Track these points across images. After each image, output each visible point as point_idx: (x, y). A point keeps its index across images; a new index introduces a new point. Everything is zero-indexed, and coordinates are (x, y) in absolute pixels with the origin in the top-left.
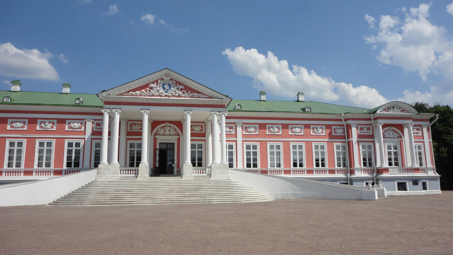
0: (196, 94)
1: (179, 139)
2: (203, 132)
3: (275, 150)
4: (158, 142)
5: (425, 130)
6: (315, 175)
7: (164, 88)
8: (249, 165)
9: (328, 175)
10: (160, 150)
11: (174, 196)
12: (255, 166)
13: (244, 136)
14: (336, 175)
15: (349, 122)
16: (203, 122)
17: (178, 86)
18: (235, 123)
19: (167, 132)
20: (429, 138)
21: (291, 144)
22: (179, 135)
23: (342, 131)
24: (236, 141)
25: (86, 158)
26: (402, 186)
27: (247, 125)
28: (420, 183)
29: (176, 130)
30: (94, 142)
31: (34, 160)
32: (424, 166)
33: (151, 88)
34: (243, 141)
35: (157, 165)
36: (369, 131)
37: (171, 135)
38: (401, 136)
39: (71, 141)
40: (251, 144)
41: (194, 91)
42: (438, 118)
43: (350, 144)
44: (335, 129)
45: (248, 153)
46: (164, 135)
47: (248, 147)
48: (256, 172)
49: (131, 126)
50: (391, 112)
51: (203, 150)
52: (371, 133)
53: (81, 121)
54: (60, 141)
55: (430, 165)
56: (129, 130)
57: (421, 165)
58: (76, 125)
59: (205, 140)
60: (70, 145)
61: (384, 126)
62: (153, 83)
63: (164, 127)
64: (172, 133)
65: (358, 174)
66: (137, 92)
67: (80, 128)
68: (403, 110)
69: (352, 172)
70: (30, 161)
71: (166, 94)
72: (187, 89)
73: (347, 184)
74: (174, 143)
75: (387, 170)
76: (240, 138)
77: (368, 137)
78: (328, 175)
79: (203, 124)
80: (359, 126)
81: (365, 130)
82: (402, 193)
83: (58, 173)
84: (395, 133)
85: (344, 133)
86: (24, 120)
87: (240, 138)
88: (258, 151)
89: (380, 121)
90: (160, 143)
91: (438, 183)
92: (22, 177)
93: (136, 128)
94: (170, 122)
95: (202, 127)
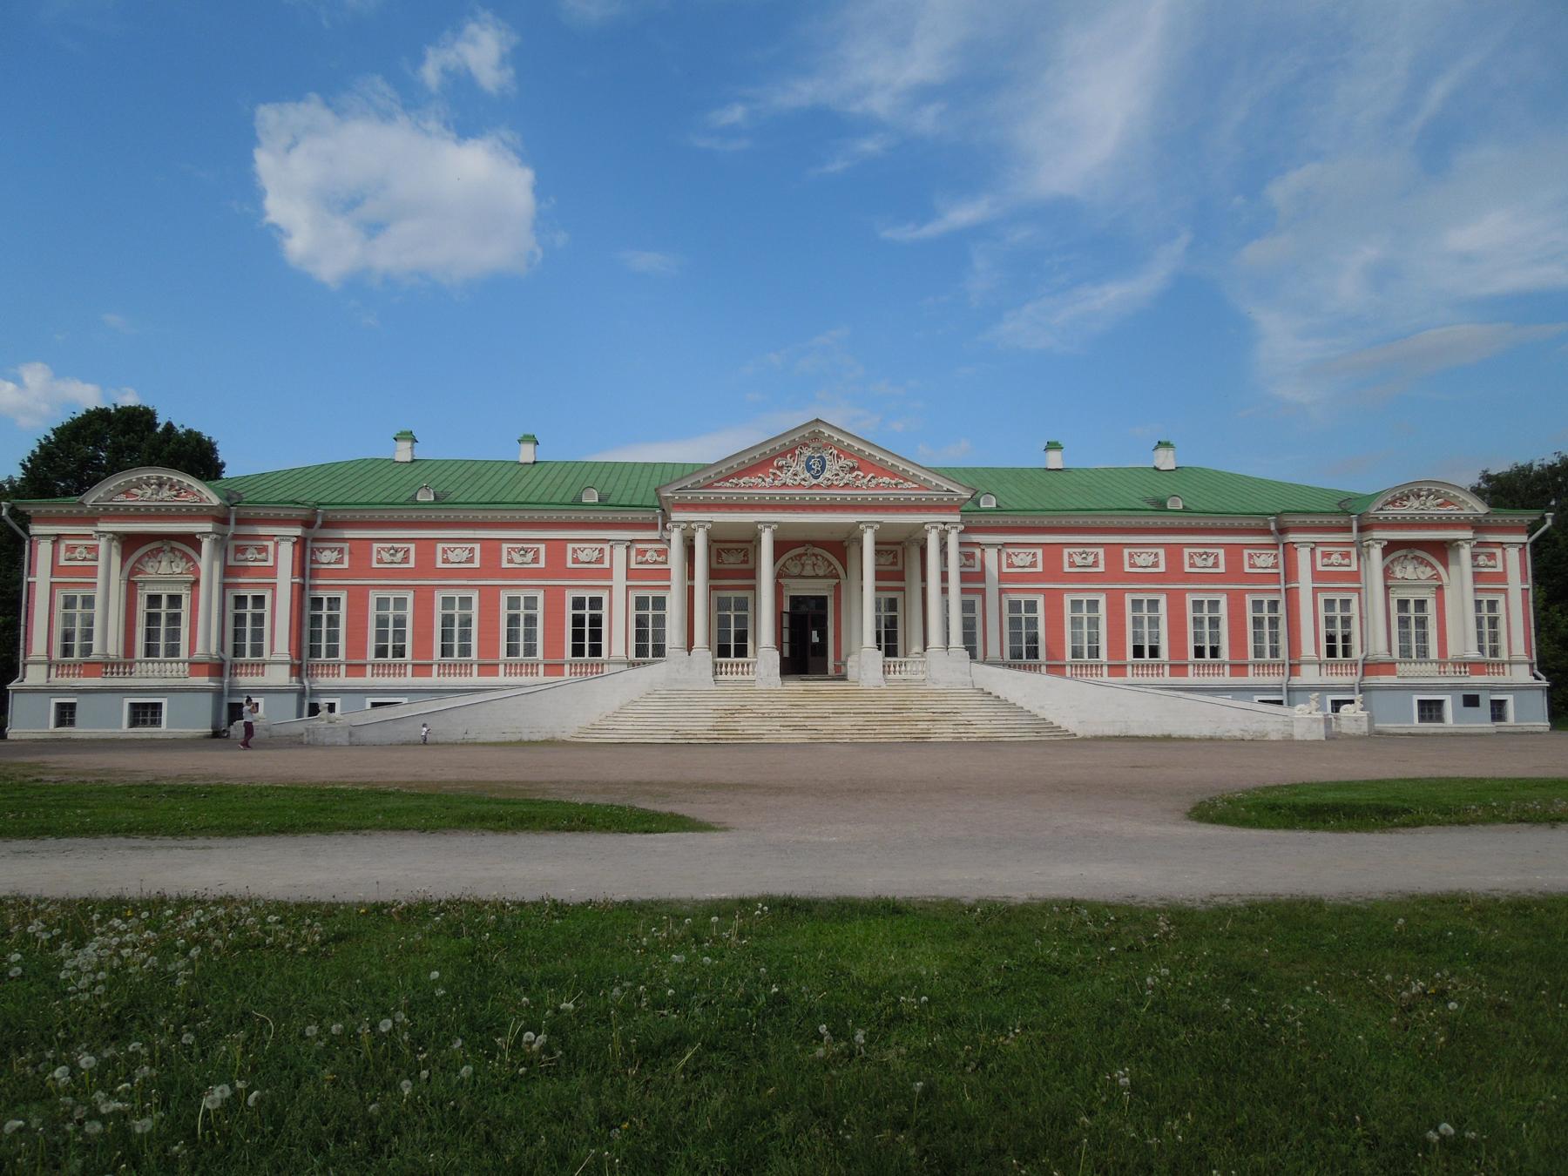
0: (886, 479)
1: (837, 588)
2: (899, 567)
3: (1085, 614)
4: (787, 594)
5: (1513, 554)
7: (809, 468)
8: (1016, 655)
9: (1226, 679)
10: (792, 615)
14: (1251, 679)
15: (1292, 537)
16: (899, 543)
17: (842, 462)
18: (979, 544)
19: (808, 571)
20: (1524, 580)
21: (1128, 598)
22: (837, 577)
23: (1271, 561)
24: (983, 592)
25: (618, 637)
26: (1431, 710)
27: (1010, 551)
28: (1485, 708)
29: (830, 564)
30: (633, 595)
31: (498, 640)
32: (1504, 656)
33: (780, 468)
34: (1002, 591)
35: (786, 654)
36: (1346, 561)
37: (817, 577)
38: (1438, 573)
39: (579, 594)
41: (882, 469)
42: (1549, 522)
43: (1292, 595)
44: (1251, 556)
46: (800, 576)
48: (1036, 668)
49: (719, 555)
50: (1412, 508)
51: (899, 615)
52: (1354, 568)
53: (600, 546)
54: (554, 595)
55: (1519, 649)
56: (715, 566)
57: (1495, 652)
59: (902, 589)
60: (578, 603)
61: (1391, 547)
62: (783, 455)
63: (800, 556)
64: (821, 573)
66: (746, 479)
67: (600, 560)
69: (1294, 669)
70: (488, 645)
71: (815, 482)
72: (864, 464)
73: (1280, 703)
74: (824, 598)
75: (1388, 667)
78: (1226, 679)
79: (899, 548)
80: (1319, 550)
81: (1336, 558)
82: (1431, 727)
83: (554, 668)
84: (1422, 568)
85: (1276, 566)
86: (470, 546)
89: (1377, 534)
90: (793, 598)
91: (1540, 703)
93: (732, 562)
94: (815, 544)
95: (895, 557)
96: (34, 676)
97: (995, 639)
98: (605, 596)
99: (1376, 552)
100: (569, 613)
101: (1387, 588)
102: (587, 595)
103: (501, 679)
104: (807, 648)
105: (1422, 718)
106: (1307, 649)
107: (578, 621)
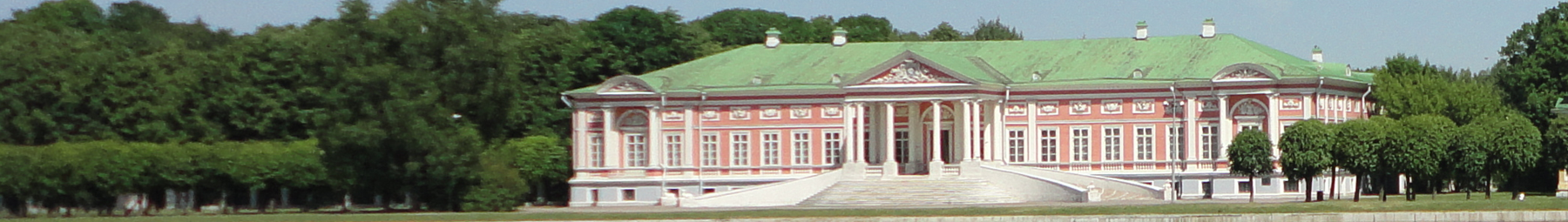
3: (1081, 137)
6: (1135, 171)
8: (1044, 158)
9: (1154, 171)
11: (903, 197)
12: (1053, 158)
13: (1038, 118)
14: (1167, 171)
40: (1049, 129)
45: (1044, 142)
47: (1044, 133)
50: (1239, 79)
58: (833, 110)
61: (1232, 100)
65: (1191, 169)
68: (1260, 75)
69: (1184, 168)
76: (1032, 122)
77: (1210, 115)
83: (817, 169)
87: (1032, 122)
88: (1057, 138)
89: (1221, 93)
92: (780, 175)
96: (580, 178)
97: (1033, 151)
98: (840, 132)
99: (1223, 104)
100: (824, 140)
101: (1235, 122)
102: (832, 132)
103: (792, 175)
104: (910, 160)
105: (1241, 190)
106: (1191, 156)
107: (828, 144)
